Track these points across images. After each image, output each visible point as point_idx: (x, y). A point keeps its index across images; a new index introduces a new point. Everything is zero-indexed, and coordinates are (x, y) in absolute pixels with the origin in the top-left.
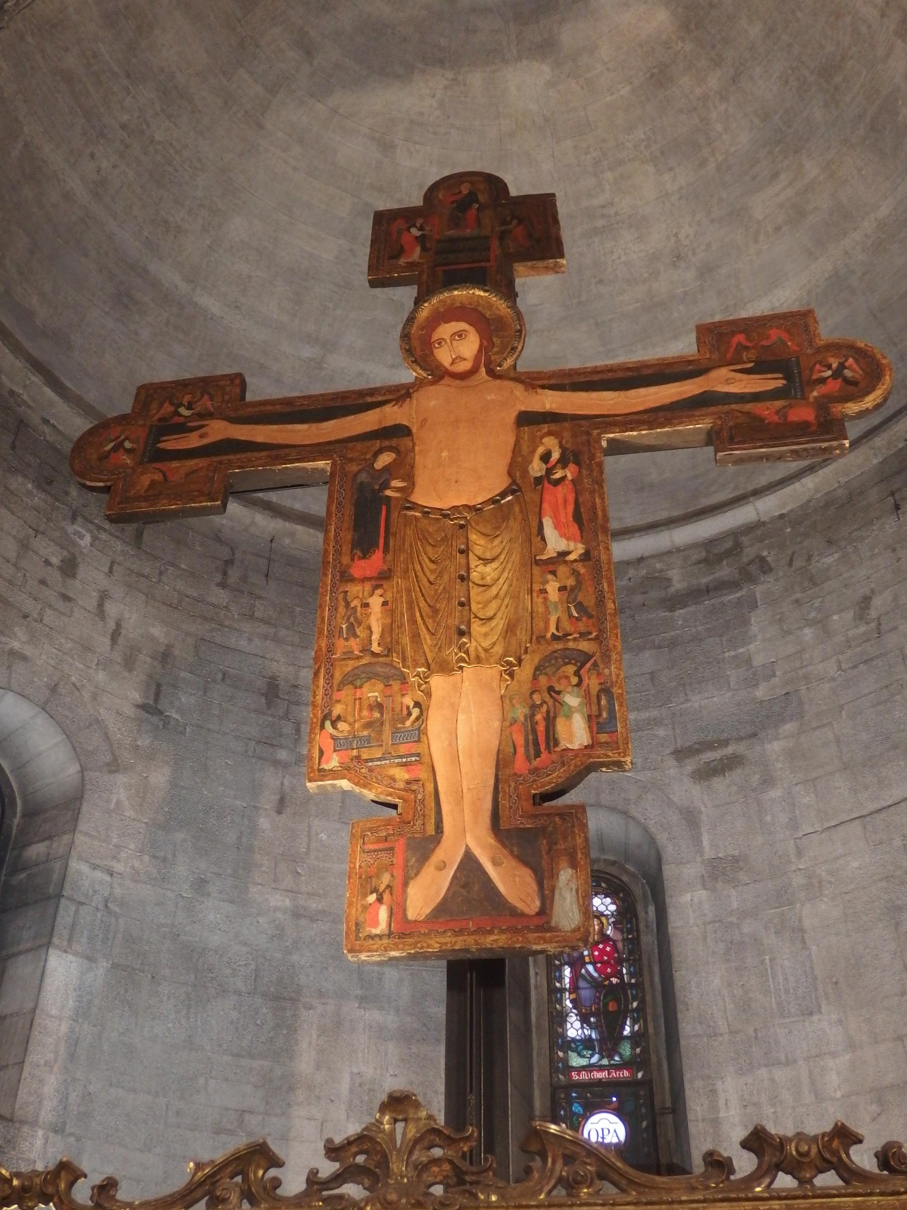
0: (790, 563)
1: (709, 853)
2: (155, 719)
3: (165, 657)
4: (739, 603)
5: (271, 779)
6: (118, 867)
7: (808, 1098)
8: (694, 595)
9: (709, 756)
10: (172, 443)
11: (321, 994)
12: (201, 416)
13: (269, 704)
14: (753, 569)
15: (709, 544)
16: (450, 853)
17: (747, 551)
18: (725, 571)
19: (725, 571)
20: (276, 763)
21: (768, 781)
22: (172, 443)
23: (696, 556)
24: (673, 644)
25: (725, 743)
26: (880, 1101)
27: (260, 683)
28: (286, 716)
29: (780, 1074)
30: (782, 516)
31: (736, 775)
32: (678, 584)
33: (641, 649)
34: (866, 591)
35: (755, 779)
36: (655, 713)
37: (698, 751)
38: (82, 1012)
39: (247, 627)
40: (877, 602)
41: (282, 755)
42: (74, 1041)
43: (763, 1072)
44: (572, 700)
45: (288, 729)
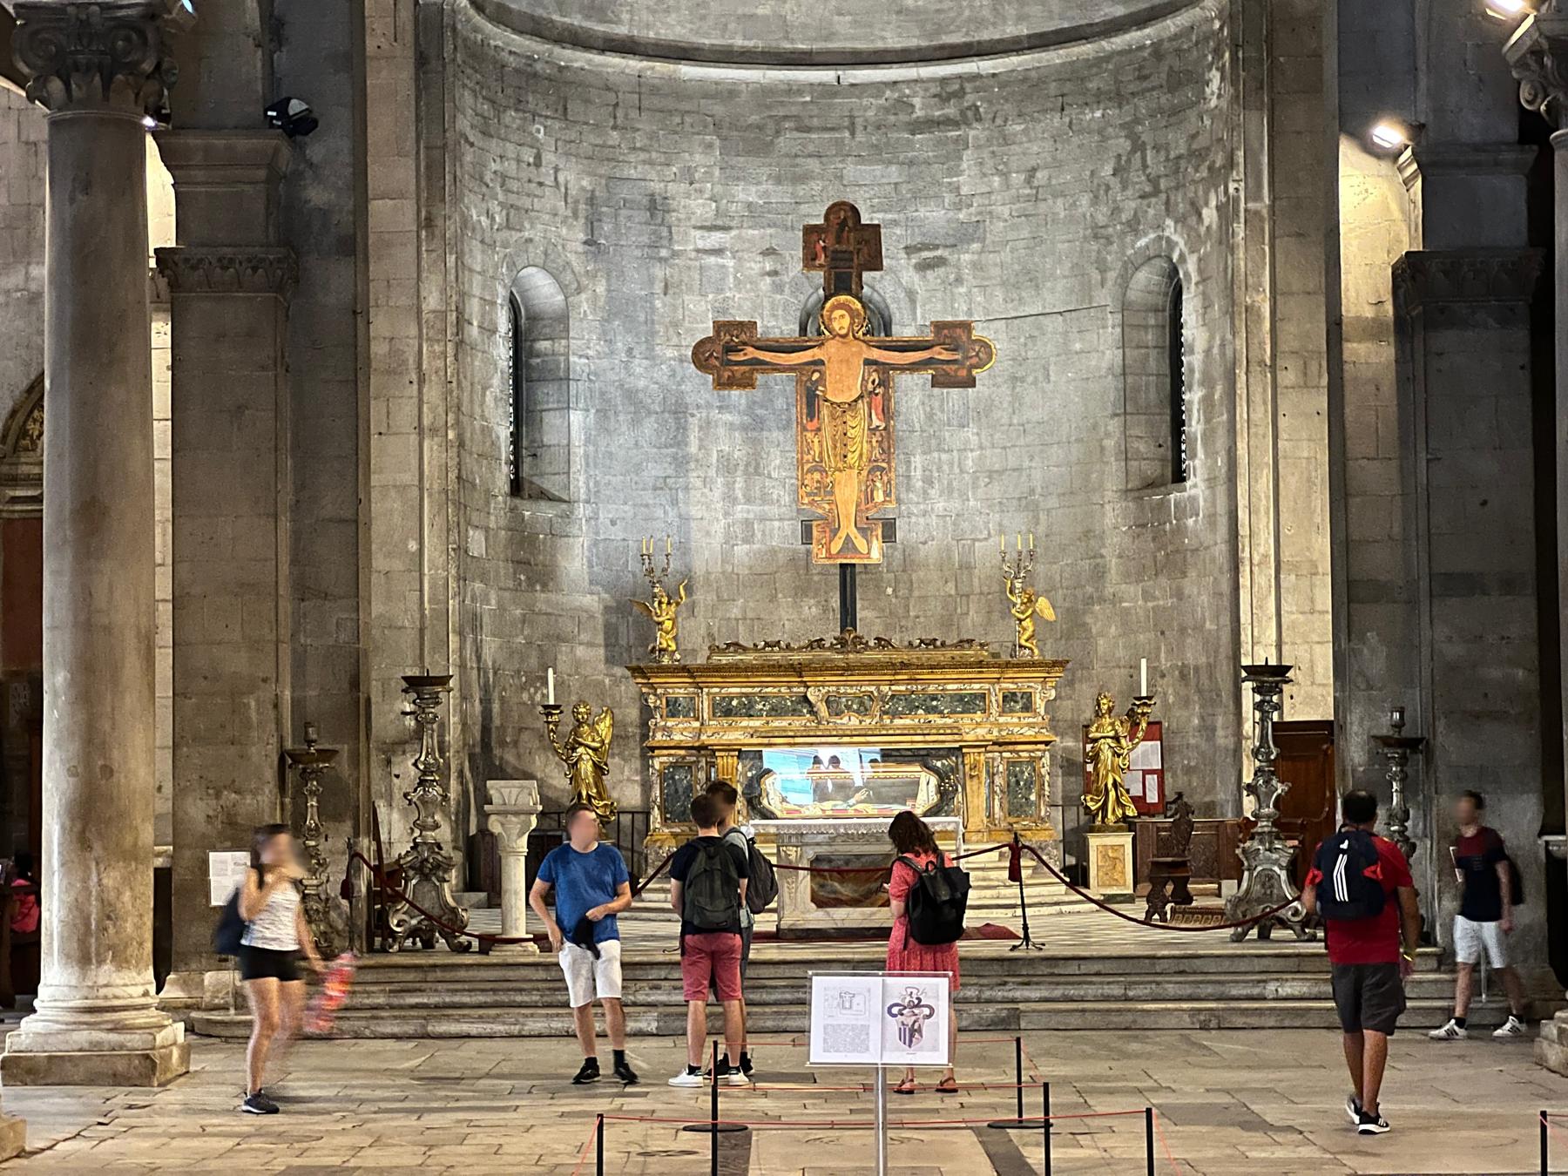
0: (994, 119)
1: (920, 321)
2: (592, 249)
3: (591, 200)
4: (957, 140)
5: (659, 272)
6: (591, 353)
7: (957, 470)
8: (930, 124)
9: (926, 254)
10: (734, 357)
11: (698, 407)
12: (745, 344)
13: (652, 215)
14: (970, 114)
15: (944, 81)
16: (842, 534)
17: (968, 97)
18: (951, 110)
19: (951, 110)
20: (661, 259)
21: (959, 280)
22: (734, 357)
23: (935, 89)
24: (911, 163)
25: (936, 247)
26: (990, 477)
27: (645, 201)
28: (662, 224)
29: (944, 456)
30: (994, 75)
31: (941, 271)
32: (919, 113)
33: (890, 163)
34: (1033, 163)
35: (952, 277)
36: (896, 216)
37: (920, 250)
38: (588, 441)
39: (632, 158)
40: (1039, 175)
41: (664, 253)
42: (586, 456)
43: (936, 455)
44: (879, 484)
45: (665, 233)
